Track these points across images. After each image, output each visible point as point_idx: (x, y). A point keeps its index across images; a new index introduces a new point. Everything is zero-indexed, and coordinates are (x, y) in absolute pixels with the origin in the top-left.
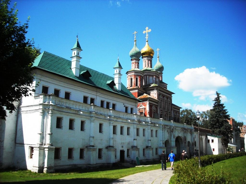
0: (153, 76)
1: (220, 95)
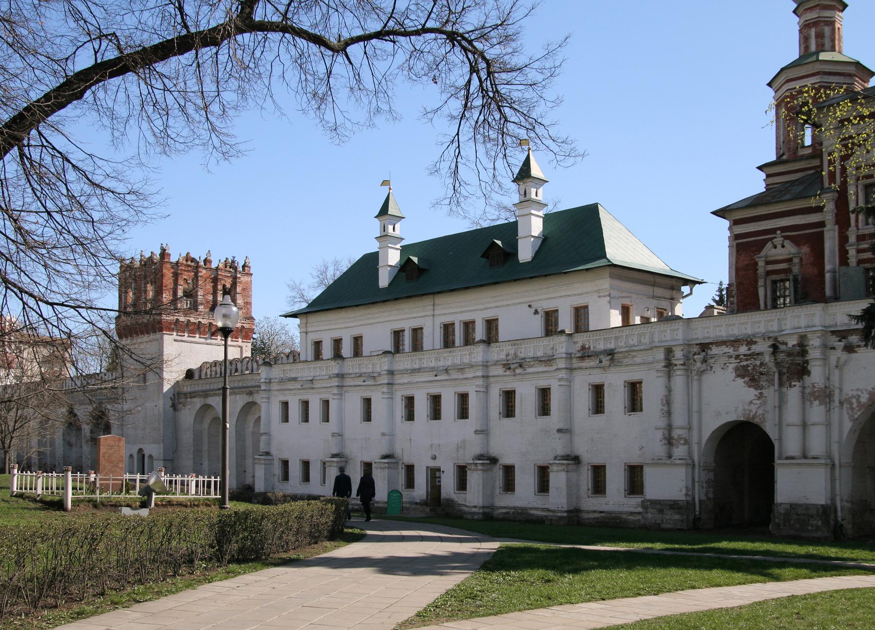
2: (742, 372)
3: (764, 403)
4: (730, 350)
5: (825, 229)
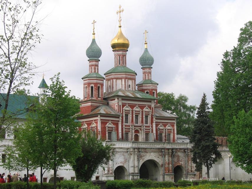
0: (121, 79)
5: (119, 122)
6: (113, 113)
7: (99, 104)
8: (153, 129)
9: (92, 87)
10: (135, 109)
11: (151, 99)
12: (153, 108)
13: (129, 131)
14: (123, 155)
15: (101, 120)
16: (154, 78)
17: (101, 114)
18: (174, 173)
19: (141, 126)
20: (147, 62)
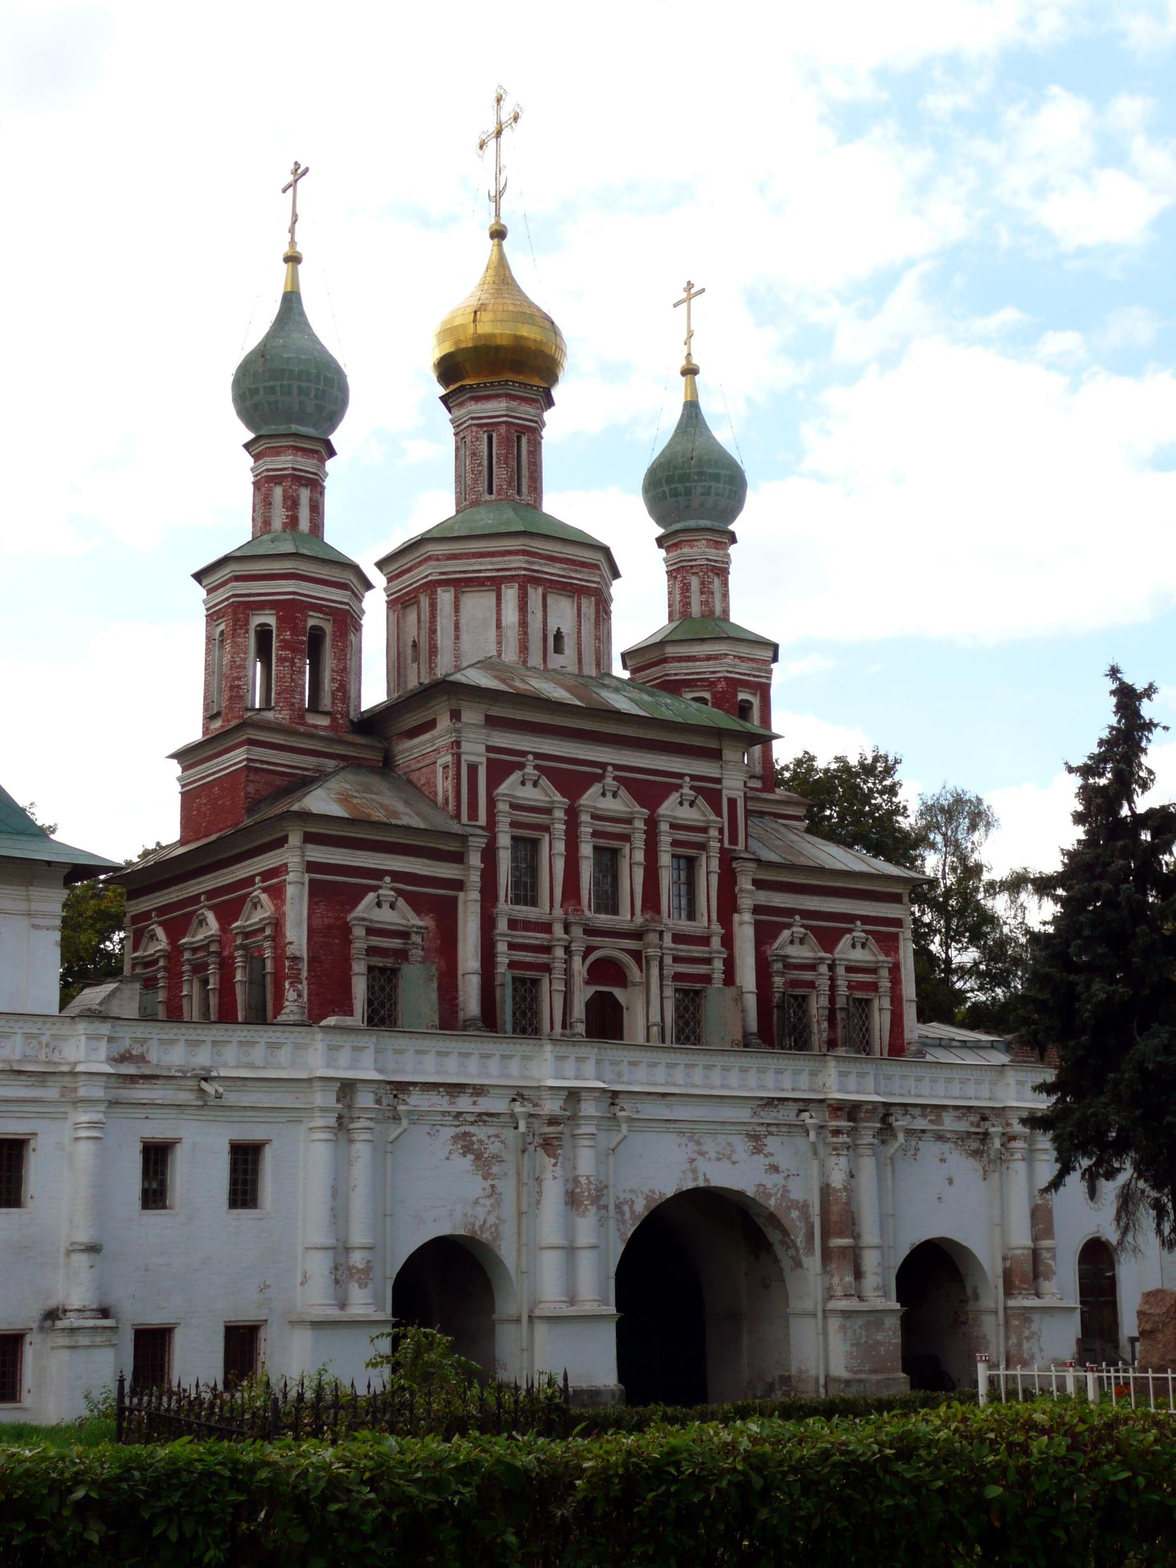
0: (495, 583)
1: (1147, 710)
2: (466, 1145)
3: (498, 1204)
4: (440, 1102)
5: (461, 895)
6: (410, 818)
7: (310, 761)
8: (738, 962)
9: (264, 634)
10: (591, 798)
11: (720, 733)
12: (732, 802)
13: (547, 968)
14: (467, 1150)
15: (312, 867)
16: (747, 610)
17: (306, 816)
18: (899, 1299)
19: (637, 935)
20: (695, 493)
